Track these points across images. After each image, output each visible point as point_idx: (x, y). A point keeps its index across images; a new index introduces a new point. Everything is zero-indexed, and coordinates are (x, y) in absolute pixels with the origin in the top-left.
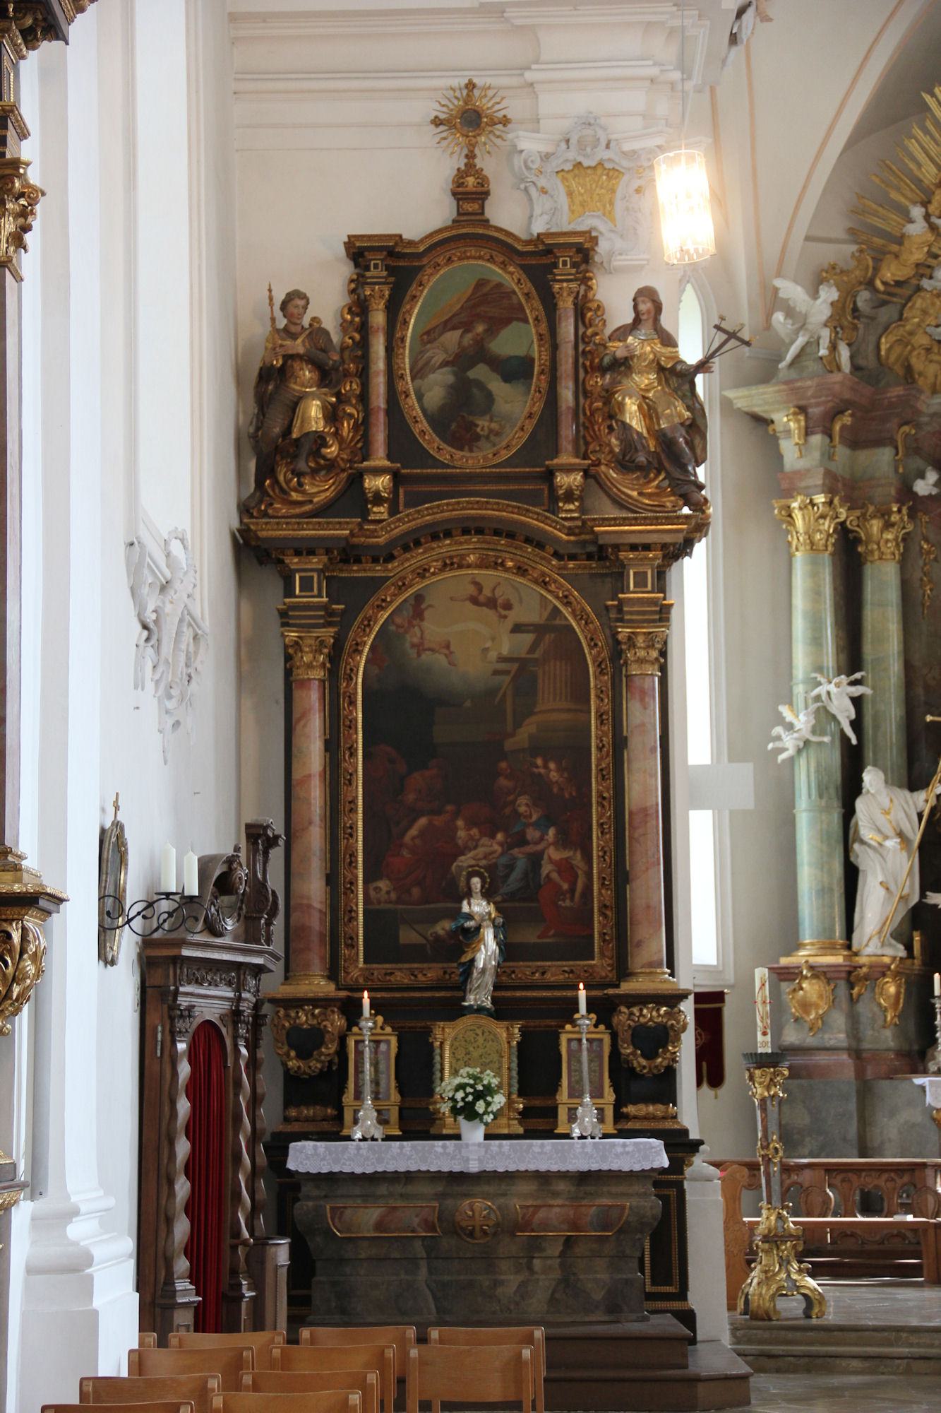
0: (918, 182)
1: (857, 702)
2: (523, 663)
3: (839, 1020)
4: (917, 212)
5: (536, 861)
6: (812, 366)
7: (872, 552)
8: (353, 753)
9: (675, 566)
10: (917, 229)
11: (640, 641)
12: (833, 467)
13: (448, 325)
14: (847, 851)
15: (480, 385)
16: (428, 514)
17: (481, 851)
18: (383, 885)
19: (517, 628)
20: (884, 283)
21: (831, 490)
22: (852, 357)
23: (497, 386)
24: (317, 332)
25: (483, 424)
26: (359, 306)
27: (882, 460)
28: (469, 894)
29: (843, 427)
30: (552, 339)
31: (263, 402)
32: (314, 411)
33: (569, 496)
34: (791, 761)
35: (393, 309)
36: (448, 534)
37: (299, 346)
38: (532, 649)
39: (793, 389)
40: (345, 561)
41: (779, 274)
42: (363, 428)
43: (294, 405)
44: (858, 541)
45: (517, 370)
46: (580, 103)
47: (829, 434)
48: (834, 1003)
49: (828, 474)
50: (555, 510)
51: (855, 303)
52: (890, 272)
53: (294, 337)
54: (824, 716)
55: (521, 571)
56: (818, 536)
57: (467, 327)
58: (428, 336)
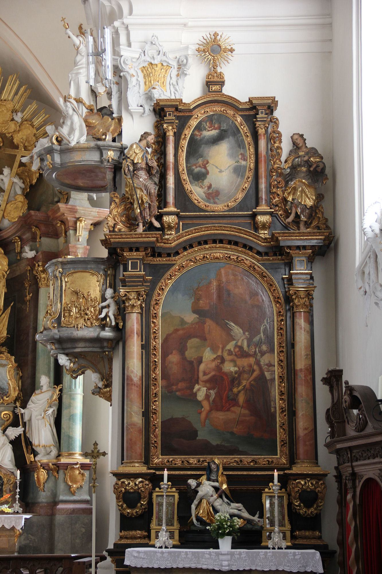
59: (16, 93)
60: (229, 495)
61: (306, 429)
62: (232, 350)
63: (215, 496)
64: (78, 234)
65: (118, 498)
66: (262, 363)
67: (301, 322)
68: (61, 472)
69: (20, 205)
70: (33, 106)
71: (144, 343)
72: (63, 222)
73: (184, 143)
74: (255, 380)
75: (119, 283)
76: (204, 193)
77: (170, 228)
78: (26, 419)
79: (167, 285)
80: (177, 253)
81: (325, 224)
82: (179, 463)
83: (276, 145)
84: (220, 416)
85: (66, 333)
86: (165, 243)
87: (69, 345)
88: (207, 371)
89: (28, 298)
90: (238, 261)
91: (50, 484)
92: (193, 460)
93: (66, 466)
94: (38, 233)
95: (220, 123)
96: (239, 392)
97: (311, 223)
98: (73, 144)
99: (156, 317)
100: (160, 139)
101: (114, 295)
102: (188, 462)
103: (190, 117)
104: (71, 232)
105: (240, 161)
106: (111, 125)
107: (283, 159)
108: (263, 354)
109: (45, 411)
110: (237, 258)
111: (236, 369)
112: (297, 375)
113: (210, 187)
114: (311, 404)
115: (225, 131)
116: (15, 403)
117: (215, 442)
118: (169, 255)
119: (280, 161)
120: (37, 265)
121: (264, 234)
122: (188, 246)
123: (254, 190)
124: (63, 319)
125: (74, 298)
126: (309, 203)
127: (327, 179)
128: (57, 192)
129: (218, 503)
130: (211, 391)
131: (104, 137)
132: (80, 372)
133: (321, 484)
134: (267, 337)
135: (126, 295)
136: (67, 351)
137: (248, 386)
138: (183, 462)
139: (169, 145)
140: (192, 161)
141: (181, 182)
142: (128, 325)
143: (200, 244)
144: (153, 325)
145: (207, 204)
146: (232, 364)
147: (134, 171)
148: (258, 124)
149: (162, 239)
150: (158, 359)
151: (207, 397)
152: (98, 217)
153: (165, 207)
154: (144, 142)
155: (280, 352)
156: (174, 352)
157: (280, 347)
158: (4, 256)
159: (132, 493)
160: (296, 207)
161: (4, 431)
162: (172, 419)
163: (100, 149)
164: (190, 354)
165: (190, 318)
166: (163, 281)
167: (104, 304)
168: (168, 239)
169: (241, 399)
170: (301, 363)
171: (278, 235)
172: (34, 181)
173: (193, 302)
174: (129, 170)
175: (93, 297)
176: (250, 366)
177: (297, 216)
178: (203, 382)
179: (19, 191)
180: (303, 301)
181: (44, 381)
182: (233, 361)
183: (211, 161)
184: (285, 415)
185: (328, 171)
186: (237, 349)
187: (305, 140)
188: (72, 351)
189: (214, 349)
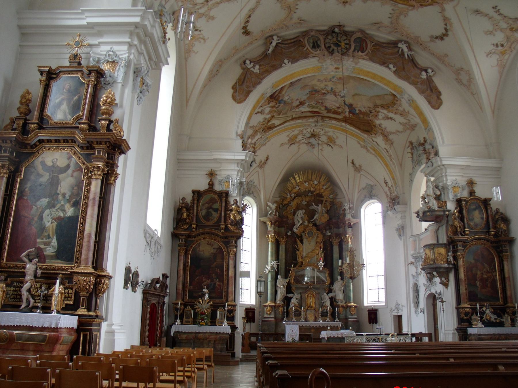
0: (289, 190)
1: (278, 265)
2: (215, 254)
3: (273, 313)
4: (289, 194)
5: (215, 284)
6: (273, 215)
8: (188, 266)
9: (238, 240)
10: (289, 196)
11: (232, 251)
13: (206, 203)
14: (275, 288)
15: (210, 212)
16: (201, 231)
17: (207, 282)
18: (192, 287)
19: (214, 249)
21: (275, 233)
22: (279, 214)
23: (213, 212)
24: (187, 204)
25: (211, 218)
26: (193, 200)
28: (204, 289)
29: (277, 224)
30: (221, 206)
31: (178, 213)
32: (185, 215)
33: (222, 229)
34: (267, 274)
35: (198, 201)
36: (204, 234)
37: (184, 205)
38: (216, 251)
39: (269, 218)
40: (188, 237)
41: (268, 202)
42: (192, 218)
43: (182, 214)
45: (216, 210)
46: (227, 173)
47: (275, 225)
48: (272, 311)
50: (220, 231)
52: (285, 202)
53: (183, 204)
54: (272, 267)
55: (215, 240)
57: (209, 204)
58: (203, 205)
59: (325, 180)
68: (348, 309)
70: (329, 184)
72: (343, 224)
73: (467, 210)
91: (344, 312)
98: (436, 209)
109: (341, 288)
172: (329, 209)
179: (324, 212)
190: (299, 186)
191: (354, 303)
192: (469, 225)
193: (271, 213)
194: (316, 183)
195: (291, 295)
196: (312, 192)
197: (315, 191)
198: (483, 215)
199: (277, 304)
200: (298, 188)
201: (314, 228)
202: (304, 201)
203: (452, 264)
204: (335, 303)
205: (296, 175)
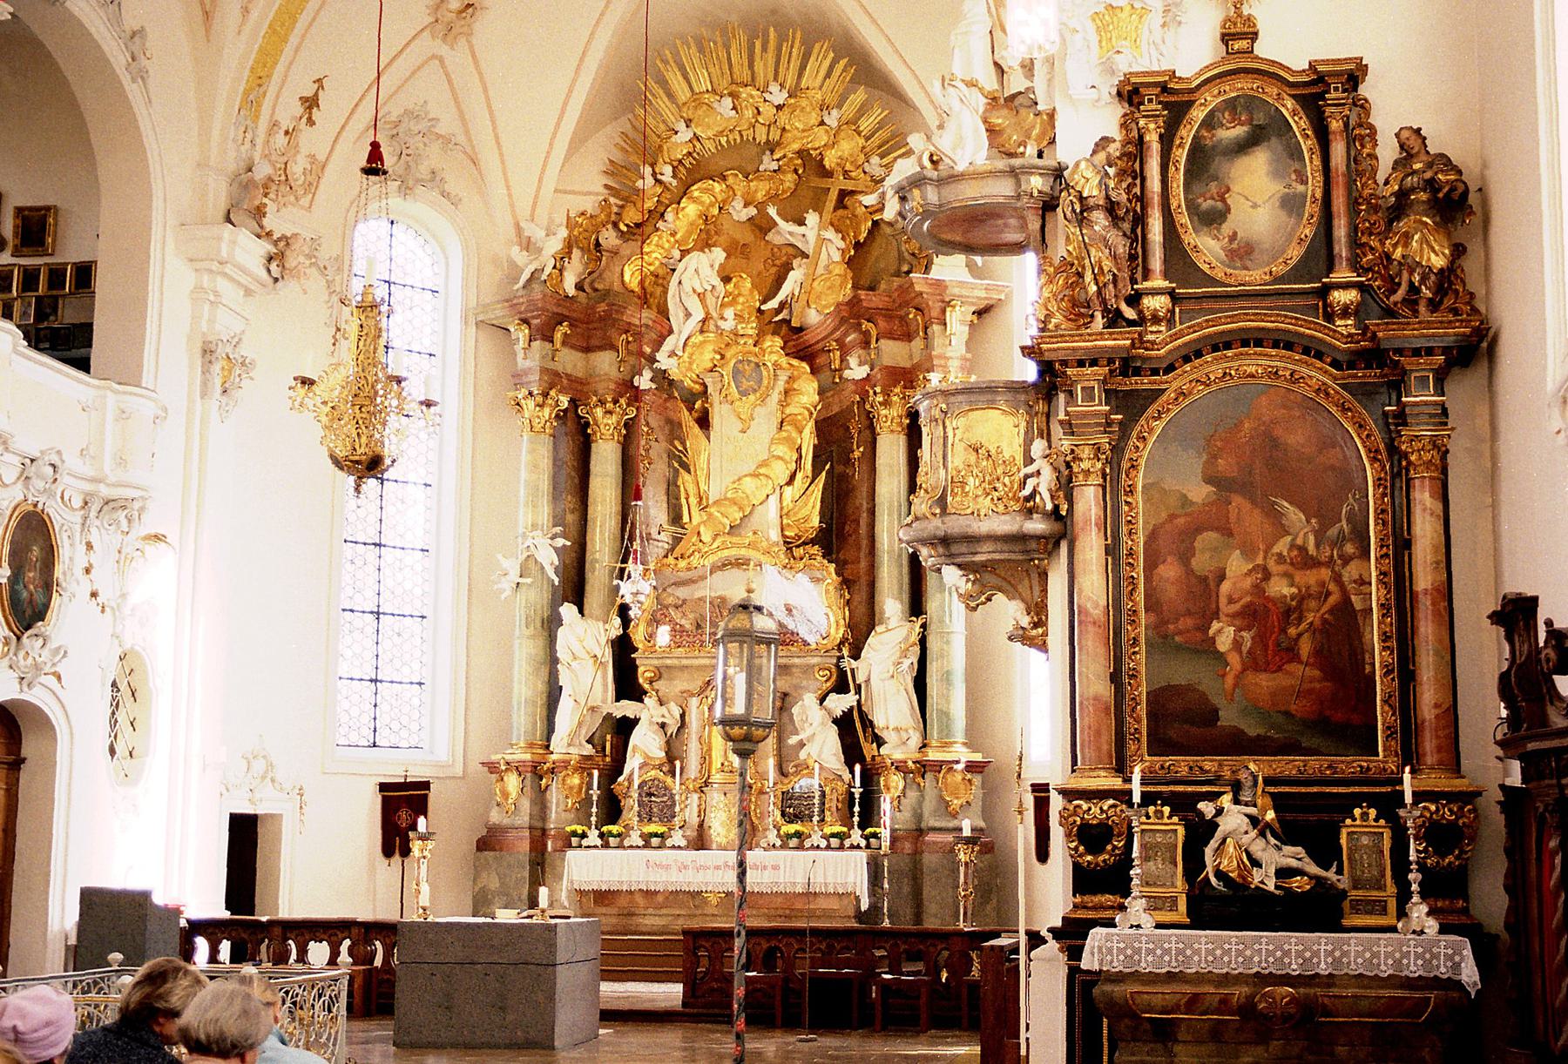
3: (526, 805)
4: (648, 170)
7: (595, 433)
12: (551, 365)
20: (627, 225)
27: (605, 364)
44: (587, 424)
49: (544, 370)
51: (597, 240)
52: (632, 216)
56: (537, 420)
59: (828, 75)
60: (1279, 831)
61: (1436, 706)
62: (1285, 553)
63: (1254, 833)
64: (948, 332)
65: (1068, 835)
66: (1345, 579)
67: (1423, 497)
69: (838, 281)
70: (859, 96)
71: (1109, 542)
73: (1181, 155)
74: (1331, 611)
75: (1057, 431)
76: (1223, 249)
77: (1156, 319)
78: (860, 679)
79: (1151, 430)
80: (1170, 368)
81: (1468, 303)
82: (1183, 771)
83: (1366, 151)
84: (1264, 682)
85: (954, 525)
86: (1147, 349)
87: (963, 548)
88: (1235, 596)
89: (857, 454)
90: (1294, 379)
92: (1209, 764)
93: (938, 766)
94: (874, 333)
95: (1251, 113)
96: (1300, 635)
97: (1441, 302)
99: (1131, 491)
100: (1131, 148)
101: (1048, 452)
102: (1201, 768)
103: (1190, 104)
104: (936, 328)
105: (1294, 184)
106: (1034, 127)
107: (1381, 178)
108: (1346, 560)
110: (1291, 375)
111: (1294, 590)
112: (1417, 602)
113: (1233, 237)
114: (1448, 658)
115: (1259, 127)
116: (840, 650)
117: (1253, 730)
118: (1155, 372)
119: (1375, 182)
120: (871, 392)
121: (1345, 325)
122: (1192, 354)
123: (1323, 239)
124: (949, 499)
125: (973, 458)
126: (1438, 262)
127: (1472, 213)
128: (906, 254)
129: (1258, 848)
130: (1244, 634)
131: (1021, 149)
132: (983, 599)
133: (1469, 811)
134: (1354, 530)
135: (1073, 451)
136: (959, 560)
137: (1317, 622)
138: (1191, 768)
139: (1149, 160)
140: (1197, 188)
141: (1175, 226)
142: (1079, 508)
143: (1215, 348)
144: (1126, 508)
145: (1229, 271)
146: (1285, 581)
147: (1082, 212)
148: (1328, 110)
149: (1142, 341)
150: (1139, 573)
151: (1237, 644)
152: (986, 298)
153: (1146, 277)
154: (1102, 156)
155: (1382, 557)
156: (1169, 559)
157: (1382, 547)
158: (811, 377)
159: (1096, 825)
160: (1411, 273)
161: (822, 700)
162: (1169, 688)
163: (1013, 173)
164: (1202, 562)
165: (1200, 492)
166: (1142, 421)
167: (1030, 469)
168: (1153, 343)
169: (1305, 647)
170: (1424, 578)
171: (1376, 328)
173: (1206, 462)
174: (1074, 210)
175: (1007, 455)
176: (1322, 584)
177: (1413, 289)
178: (1227, 615)
180: (1427, 456)
181: (892, 606)
182: (1286, 575)
183: (1235, 188)
184: (1393, 679)
185: (1473, 199)
186: (1295, 553)
187: (1425, 138)
188: (969, 559)
189: (1248, 552)
190: (688, 122)
191: (970, 745)
192: (1178, 256)
193: (529, 281)
194: (778, 96)
195: (627, 708)
196: (771, 147)
197: (778, 144)
198: (1304, 182)
199: (554, 757)
200: (684, 135)
201: (774, 343)
202: (738, 204)
203: (1046, 515)
204: (869, 749)
205: (666, 62)
